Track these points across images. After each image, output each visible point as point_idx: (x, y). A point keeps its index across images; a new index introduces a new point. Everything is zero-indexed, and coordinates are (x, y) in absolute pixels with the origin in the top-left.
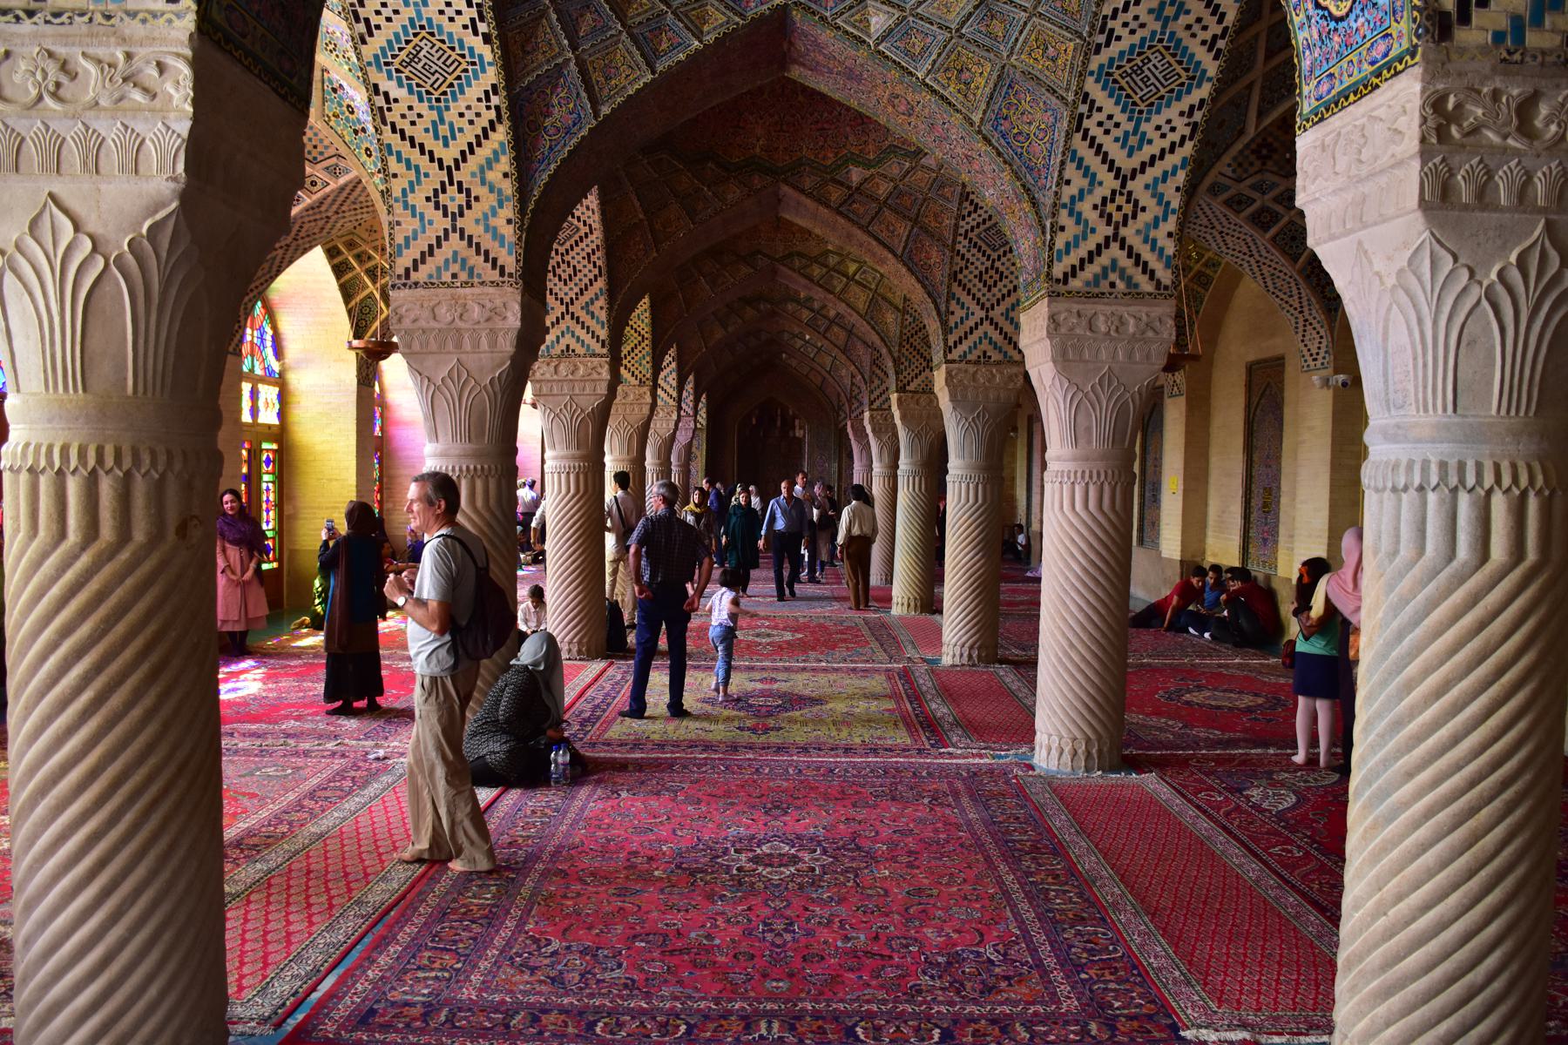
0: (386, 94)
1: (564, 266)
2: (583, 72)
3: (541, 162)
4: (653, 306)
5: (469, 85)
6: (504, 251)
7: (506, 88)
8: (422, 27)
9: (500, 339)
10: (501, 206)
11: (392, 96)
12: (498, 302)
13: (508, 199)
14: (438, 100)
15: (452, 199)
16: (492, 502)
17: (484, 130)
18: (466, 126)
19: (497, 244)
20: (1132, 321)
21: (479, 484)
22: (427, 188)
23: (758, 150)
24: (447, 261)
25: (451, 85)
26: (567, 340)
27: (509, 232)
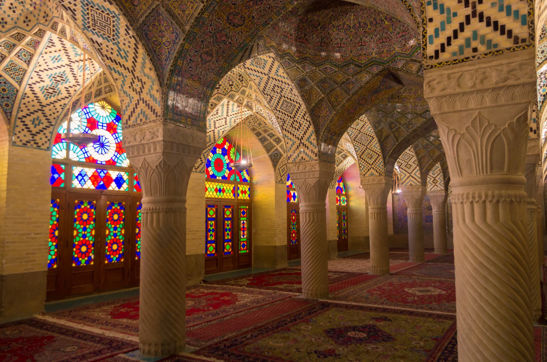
0: (97, 42)
1: (295, 123)
2: (169, 11)
3: (166, 60)
4: (379, 141)
6: (157, 105)
7: (131, 25)
8: (87, 4)
11: (99, 42)
12: (155, 129)
13: (154, 81)
15: (137, 85)
16: (161, 224)
18: (129, 49)
20: (494, 74)
21: (155, 215)
23: (374, 55)
25: (114, 31)
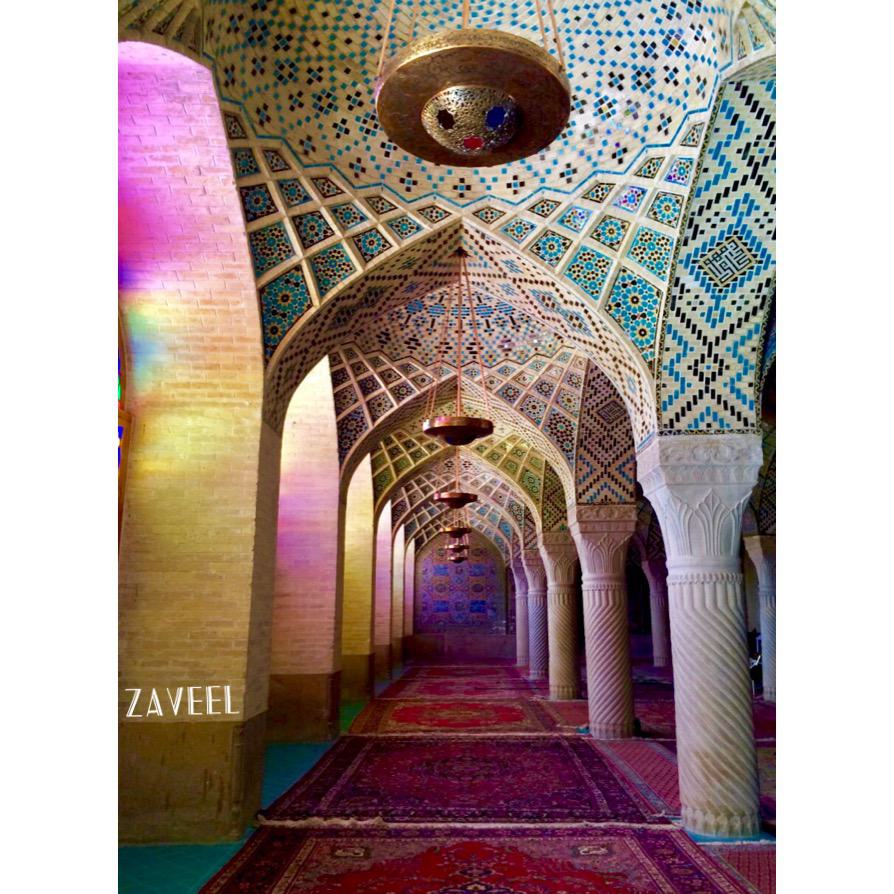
0: (683, 286)
1: (607, 439)
5: (749, 279)
6: (746, 407)
9: (745, 472)
10: (745, 373)
13: (752, 368)
14: (720, 291)
15: (708, 367)
17: (747, 315)
19: (740, 401)
21: (730, 587)
22: (690, 360)
24: (702, 415)
25: (736, 279)
26: (605, 492)
27: (750, 393)
